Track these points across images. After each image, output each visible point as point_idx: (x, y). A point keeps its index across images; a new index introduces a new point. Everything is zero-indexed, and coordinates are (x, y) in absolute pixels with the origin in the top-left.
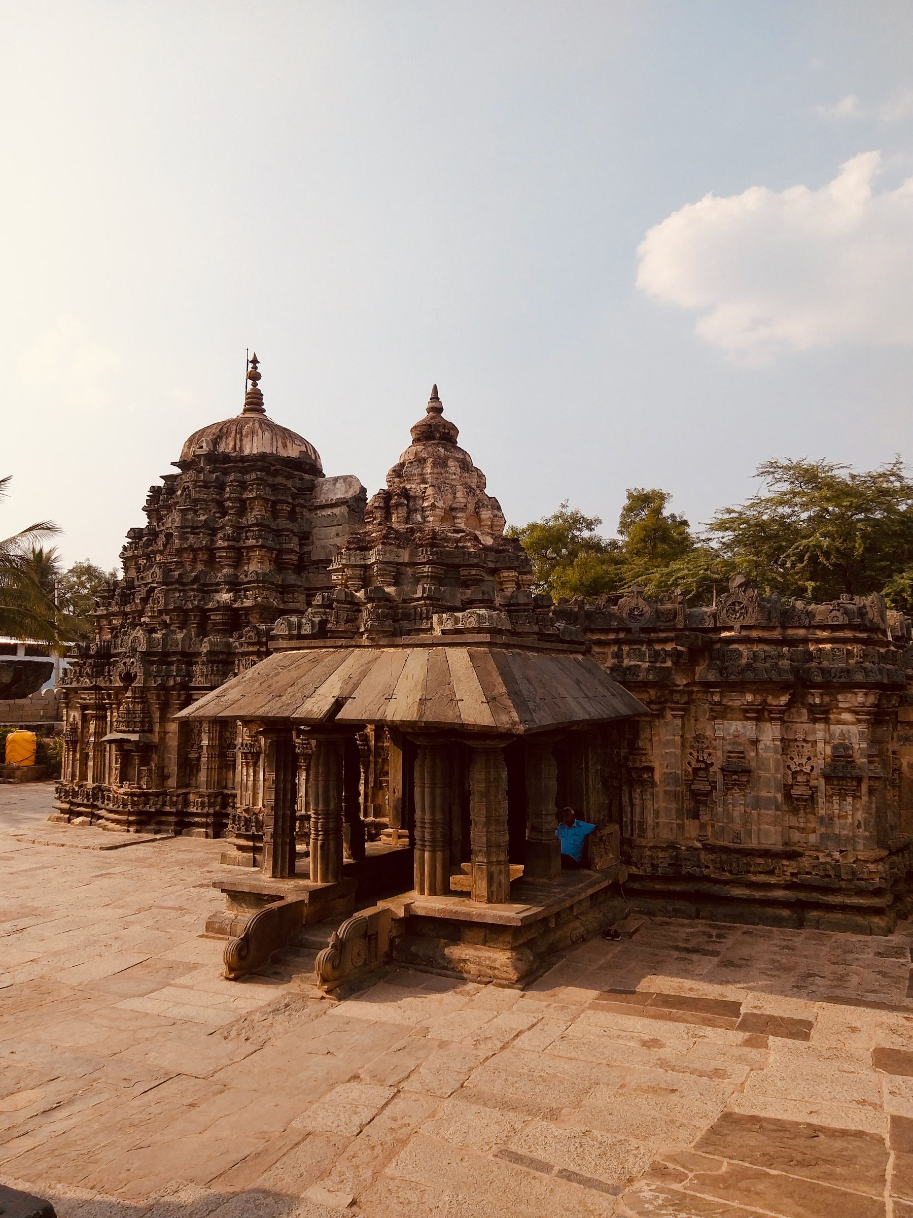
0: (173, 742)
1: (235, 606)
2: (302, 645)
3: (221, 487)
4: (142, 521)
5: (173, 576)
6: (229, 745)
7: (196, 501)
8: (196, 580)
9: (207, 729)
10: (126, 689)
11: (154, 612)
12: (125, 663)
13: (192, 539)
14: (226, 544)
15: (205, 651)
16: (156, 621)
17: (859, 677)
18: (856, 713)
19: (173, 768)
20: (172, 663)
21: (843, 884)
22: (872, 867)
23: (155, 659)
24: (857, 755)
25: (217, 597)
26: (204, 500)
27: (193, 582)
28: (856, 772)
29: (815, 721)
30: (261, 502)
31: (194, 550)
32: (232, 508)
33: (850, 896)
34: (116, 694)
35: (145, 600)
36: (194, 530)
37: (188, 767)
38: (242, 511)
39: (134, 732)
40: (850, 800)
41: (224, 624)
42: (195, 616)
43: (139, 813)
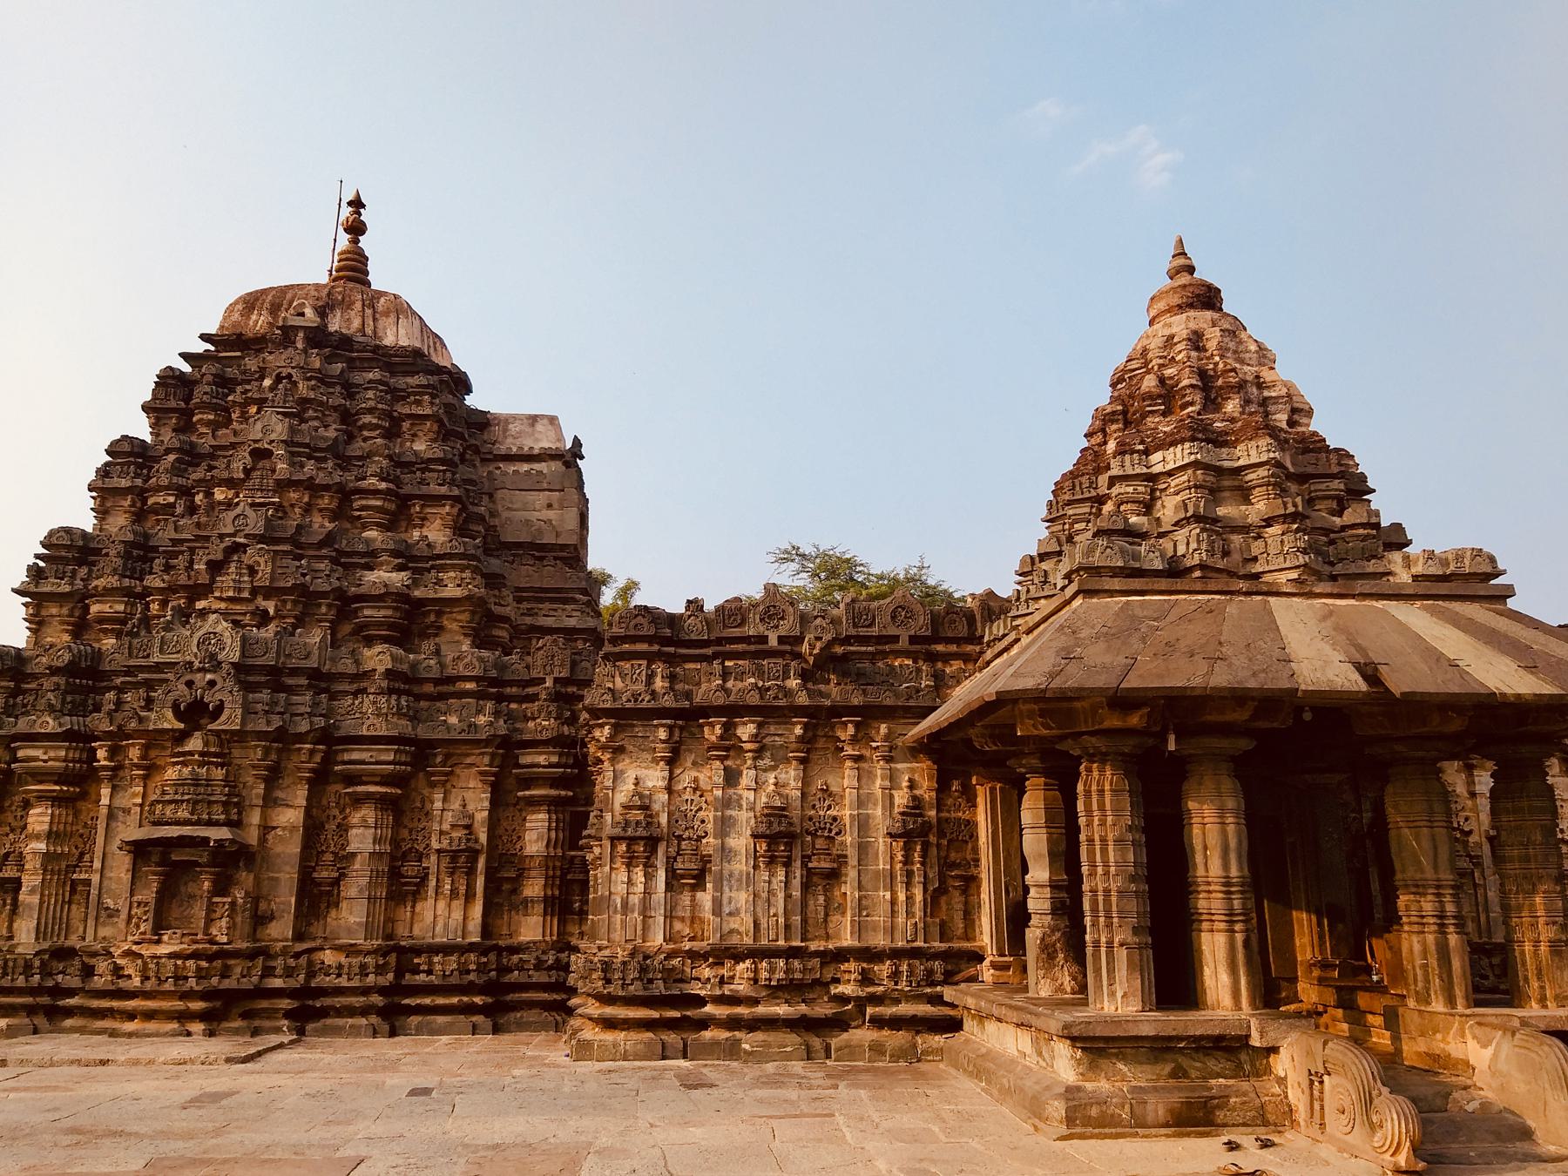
0: (288, 848)
1: (417, 593)
2: (1156, 587)
3: (350, 390)
4: (142, 429)
5: (284, 528)
6: (404, 855)
7: (304, 402)
8: (329, 540)
9: (371, 821)
10: (181, 737)
11: (240, 590)
13: (310, 467)
14: (383, 485)
15: (381, 669)
16: (238, 607)
19: (286, 898)
20: (290, 690)
23: (263, 679)
25: (372, 577)
26: (321, 404)
27: (321, 544)
30: (435, 427)
31: (310, 486)
32: (377, 427)
34: (146, 748)
35: (216, 567)
36: (313, 452)
37: (316, 898)
38: (392, 433)
39: (210, 823)
41: (391, 626)
42: (329, 606)
43: (205, 996)
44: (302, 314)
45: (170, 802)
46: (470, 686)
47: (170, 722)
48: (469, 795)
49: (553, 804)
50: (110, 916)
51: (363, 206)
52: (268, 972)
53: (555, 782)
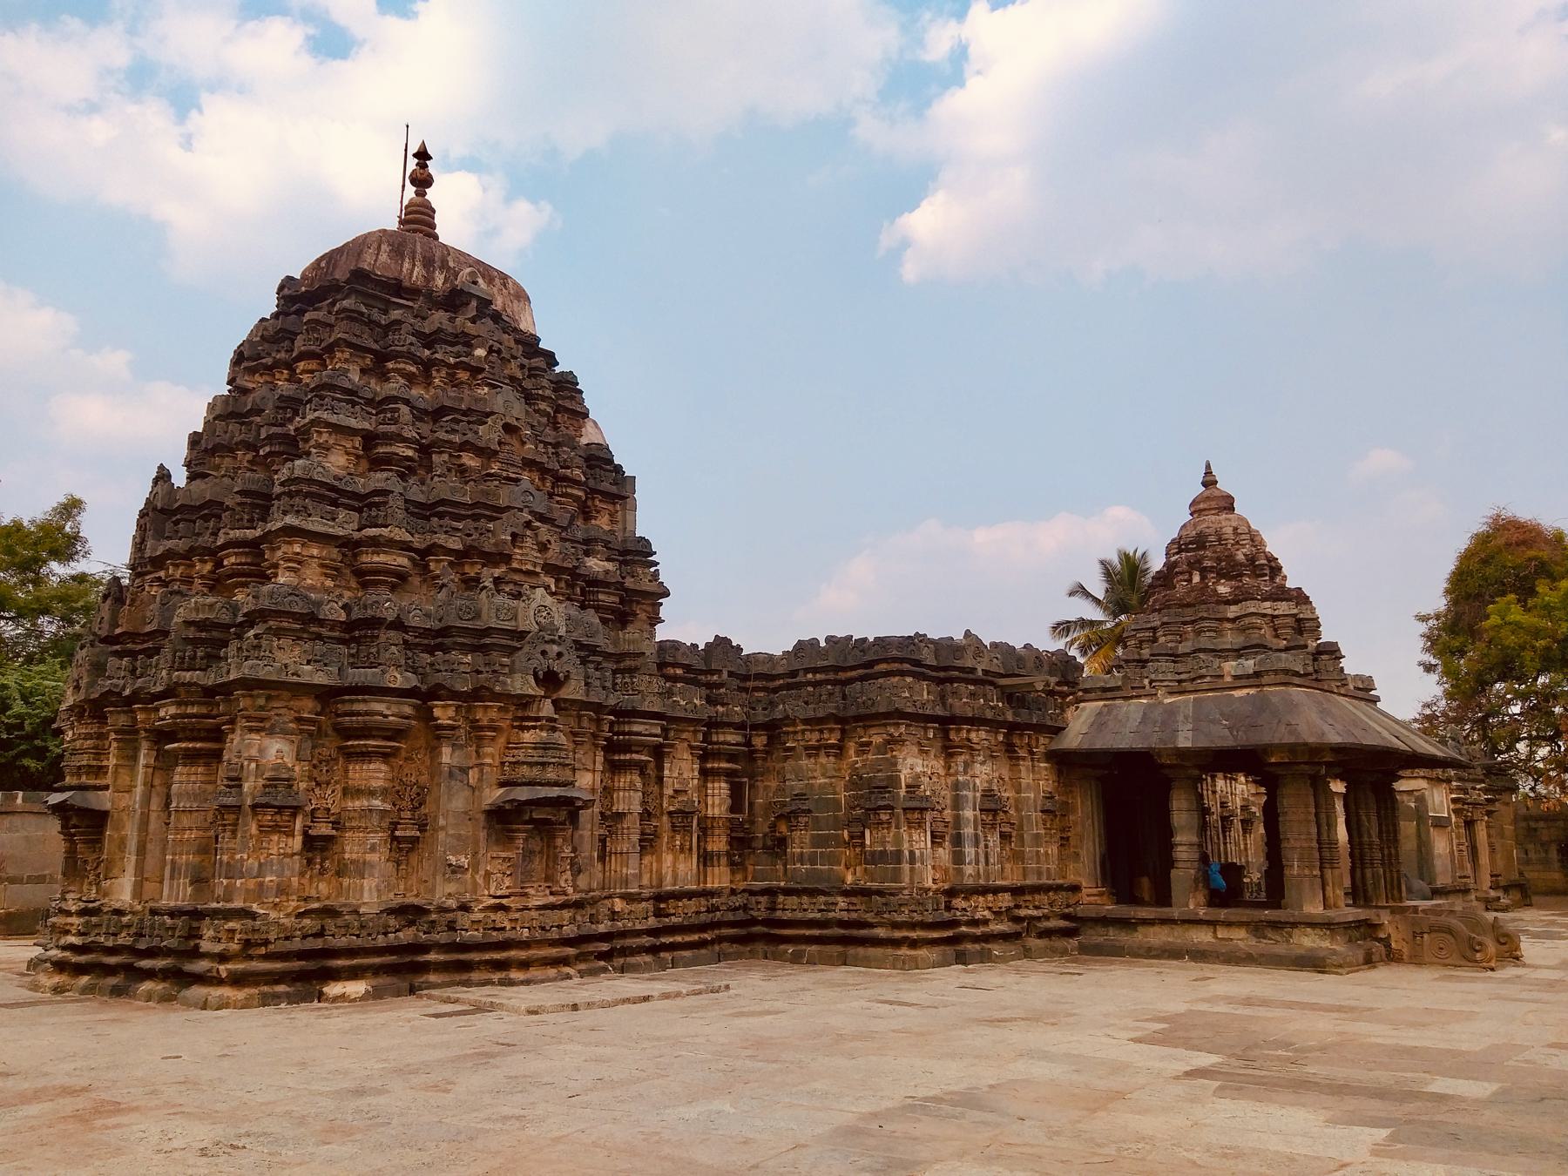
12: (544, 653)
44: (475, 283)
45: (537, 763)
46: (679, 671)
47: (531, 688)
48: (684, 765)
49: (730, 774)
50: (454, 872)
51: (430, 158)
52: (593, 919)
53: (732, 758)
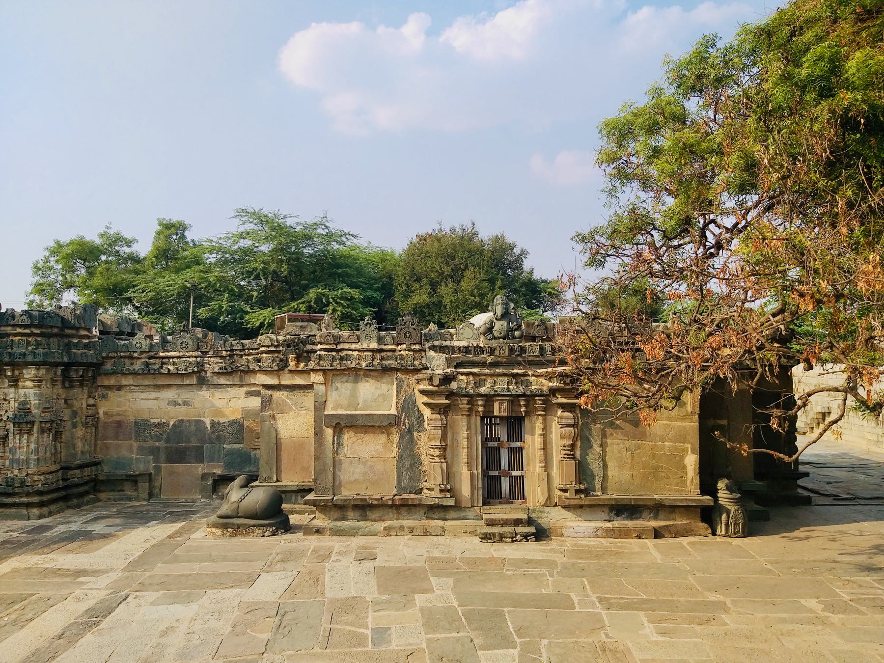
17: (30, 358)
18: (33, 381)
21: (16, 490)
22: (36, 478)
24: (32, 408)
28: (30, 419)
29: (11, 386)
33: (21, 497)
40: (25, 436)
